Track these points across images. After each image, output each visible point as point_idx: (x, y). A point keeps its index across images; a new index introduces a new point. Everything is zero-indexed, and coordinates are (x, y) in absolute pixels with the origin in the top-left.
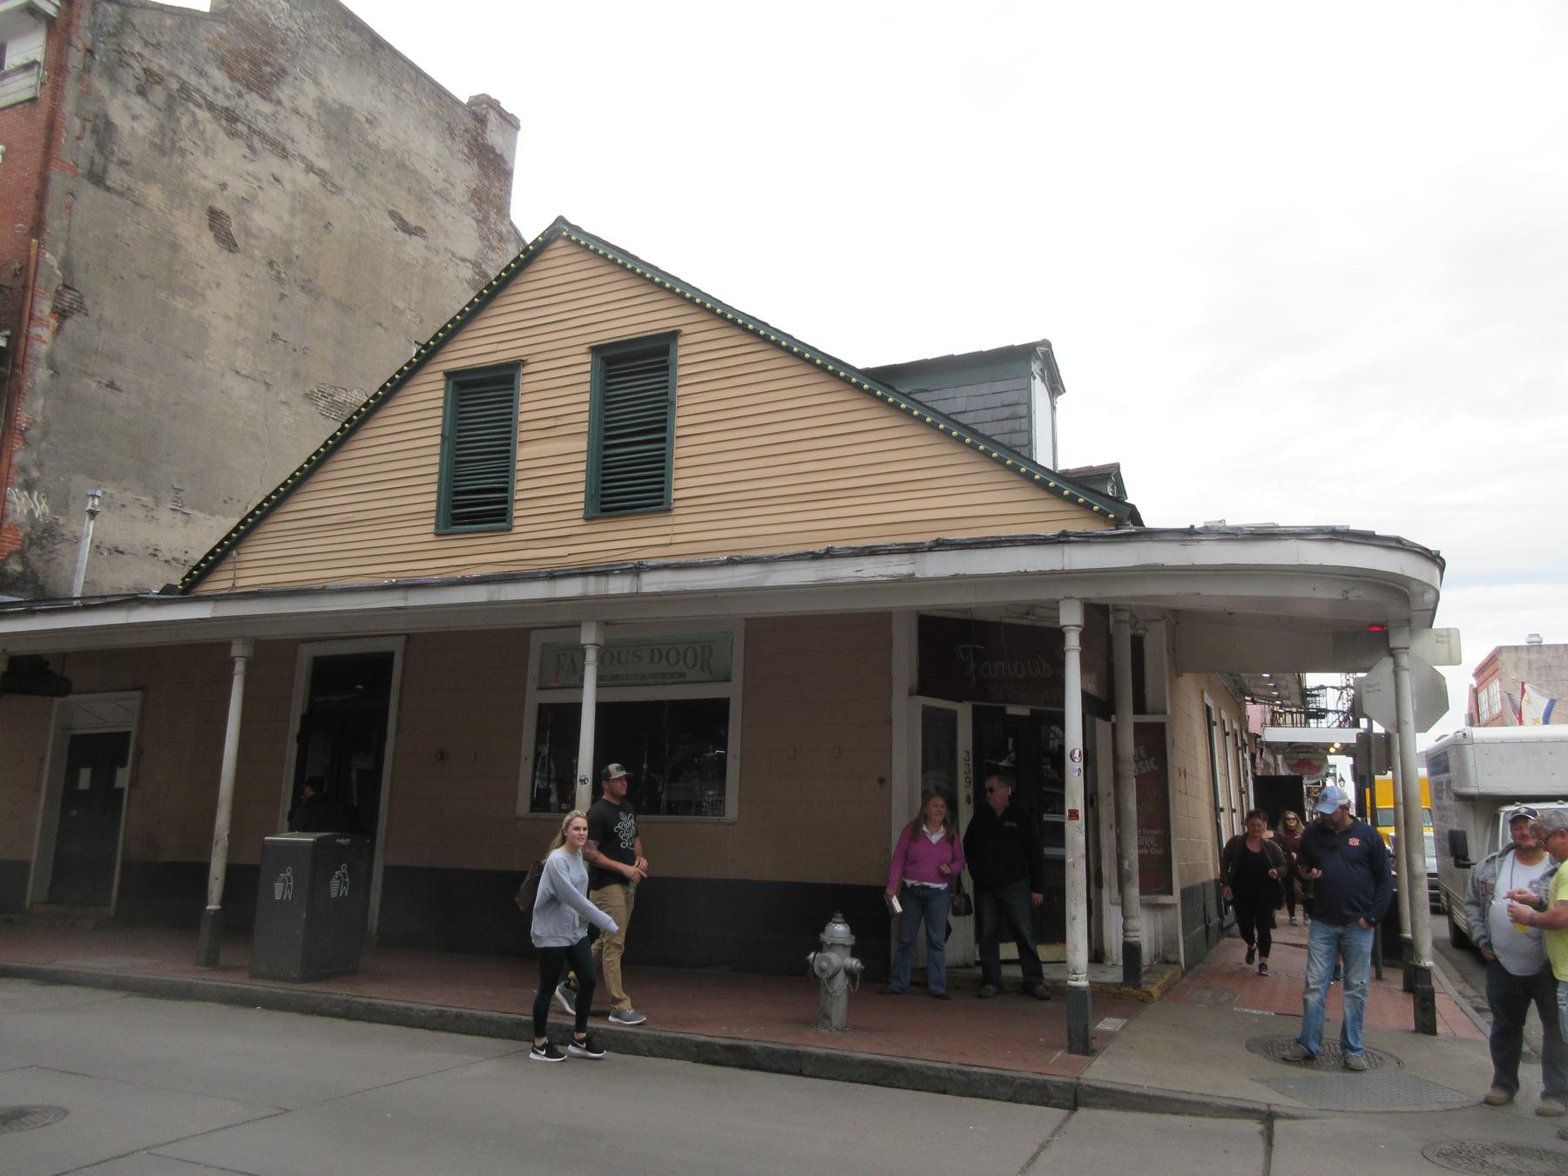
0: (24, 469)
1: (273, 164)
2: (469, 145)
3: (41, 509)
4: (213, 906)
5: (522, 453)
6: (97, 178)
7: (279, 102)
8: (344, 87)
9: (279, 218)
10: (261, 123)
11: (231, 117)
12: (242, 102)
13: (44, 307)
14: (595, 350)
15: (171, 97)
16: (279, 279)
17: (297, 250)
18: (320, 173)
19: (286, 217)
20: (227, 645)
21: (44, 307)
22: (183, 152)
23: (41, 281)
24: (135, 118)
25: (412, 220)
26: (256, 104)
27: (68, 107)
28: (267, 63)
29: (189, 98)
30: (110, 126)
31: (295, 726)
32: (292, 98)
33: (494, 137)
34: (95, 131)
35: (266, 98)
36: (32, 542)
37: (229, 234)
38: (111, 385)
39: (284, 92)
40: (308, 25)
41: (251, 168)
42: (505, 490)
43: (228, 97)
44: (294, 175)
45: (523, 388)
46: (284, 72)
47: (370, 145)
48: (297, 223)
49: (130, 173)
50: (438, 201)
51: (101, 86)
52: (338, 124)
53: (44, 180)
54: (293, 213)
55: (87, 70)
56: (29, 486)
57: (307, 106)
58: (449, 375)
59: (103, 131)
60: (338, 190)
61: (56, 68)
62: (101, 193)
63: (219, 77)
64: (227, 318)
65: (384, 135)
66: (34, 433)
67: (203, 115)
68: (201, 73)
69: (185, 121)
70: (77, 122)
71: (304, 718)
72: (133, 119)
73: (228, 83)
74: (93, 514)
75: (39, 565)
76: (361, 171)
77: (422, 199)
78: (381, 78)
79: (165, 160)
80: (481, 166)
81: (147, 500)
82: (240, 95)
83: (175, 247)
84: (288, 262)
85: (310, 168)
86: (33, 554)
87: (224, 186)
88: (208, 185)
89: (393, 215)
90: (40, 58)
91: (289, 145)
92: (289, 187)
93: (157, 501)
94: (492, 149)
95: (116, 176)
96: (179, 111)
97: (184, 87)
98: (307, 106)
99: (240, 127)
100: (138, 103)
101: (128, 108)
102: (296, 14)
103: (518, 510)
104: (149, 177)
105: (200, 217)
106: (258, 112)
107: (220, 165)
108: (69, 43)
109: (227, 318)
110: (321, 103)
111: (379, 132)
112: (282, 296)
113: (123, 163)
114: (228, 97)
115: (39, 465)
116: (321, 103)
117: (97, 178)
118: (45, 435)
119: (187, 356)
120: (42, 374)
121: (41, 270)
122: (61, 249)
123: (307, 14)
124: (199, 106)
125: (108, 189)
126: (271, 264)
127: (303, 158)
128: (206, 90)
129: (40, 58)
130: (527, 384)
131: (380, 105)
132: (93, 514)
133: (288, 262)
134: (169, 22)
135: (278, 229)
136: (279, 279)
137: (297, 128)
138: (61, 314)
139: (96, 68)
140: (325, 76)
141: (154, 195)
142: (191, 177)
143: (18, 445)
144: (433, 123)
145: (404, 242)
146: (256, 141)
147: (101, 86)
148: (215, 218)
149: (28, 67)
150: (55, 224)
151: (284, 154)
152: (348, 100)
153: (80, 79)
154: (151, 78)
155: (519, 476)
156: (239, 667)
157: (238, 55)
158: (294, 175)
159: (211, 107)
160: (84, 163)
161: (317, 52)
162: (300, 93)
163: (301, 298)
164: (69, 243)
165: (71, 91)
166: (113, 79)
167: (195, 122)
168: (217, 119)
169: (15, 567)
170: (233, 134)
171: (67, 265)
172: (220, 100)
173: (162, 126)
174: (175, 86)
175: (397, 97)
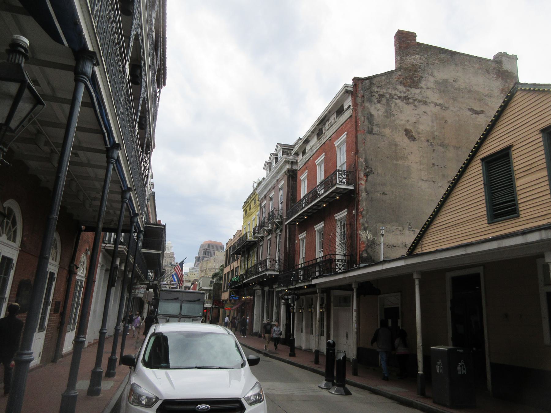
0: (363, 224)
1: (423, 108)
2: (496, 74)
3: (370, 236)
4: (420, 372)
5: (518, 183)
6: (370, 132)
7: (422, 88)
8: (443, 73)
9: (428, 125)
10: (417, 97)
11: (407, 98)
12: (409, 92)
13: (362, 175)
14: (543, 131)
15: (388, 100)
16: (432, 145)
17: (436, 133)
18: (440, 105)
19: (430, 124)
20: (411, 275)
21: (362, 175)
22: (394, 115)
23: (360, 167)
24: (378, 110)
25: (478, 109)
26: (414, 91)
27: (360, 115)
28: (415, 77)
29: (393, 98)
30: (371, 115)
31: (449, 304)
32: (426, 85)
33: (506, 66)
34: (368, 118)
35: (417, 88)
36: (369, 247)
37: (412, 136)
38: (384, 193)
39: (423, 84)
40: (427, 59)
41: (416, 112)
42: (514, 200)
43: (405, 93)
45: (514, 157)
46: (422, 77)
47: (456, 89)
48: (435, 125)
49: (379, 127)
50: (487, 98)
51: (367, 105)
52: (443, 86)
53: (356, 137)
54: (433, 122)
55: (363, 102)
56: (365, 229)
58: (482, 160)
59: (370, 117)
60: (447, 108)
61: (355, 104)
62: (372, 136)
63: (401, 88)
64: (416, 163)
65: (461, 84)
66: (364, 213)
67: (398, 101)
68: (395, 89)
69: (393, 105)
70: (363, 118)
71: (451, 301)
72: (377, 110)
73: (404, 89)
74: (383, 235)
75: (371, 254)
76: (454, 99)
77: (480, 100)
78: (456, 64)
79: (389, 119)
80: (503, 79)
81: (400, 228)
82: (408, 91)
83: (396, 145)
84: (434, 138)
85: (436, 105)
86: (369, 250)
87: (408, 121)
88: (403, 122)
89: (470, 110)
90: (351, 104)
91: (427, 100)
92: (430, 114)
93: (403, 228)
94: (507, 71)
95: (376, 130)
96: (390, 103)
97: (391, 96)
98: (431, 85)
99: (411, 101)
100: (378, 106)
101: (376, 108)
102: (422, 57)
103: (521, 207)
104: (385, 126)
105: (402, 132)
106: (415, 94)
107: (406, 115)
108: (357, 96)
109: (416, 163)
110: (436, 82)
111: (459, 83)
112: (434, 150)
113: (377, 125)
114: (405, 93)
115: (367, 222)
116: (436, 82)
117: (370, 132)
118: (367, 213)
119: (405, 179)
120: (364, 195)
121: (359, 164)
122: (364, 156)
123: (426, 56)
124: (396, 99)
125: (374, 134)
126: (428, 141)
127: (433, 102)
128: (398, 93)
129: (351, 104)
130: (515, 154)
131: (457, 74)
132: (383, 235)
133: (434, 138)
134: (383, 78)
135: (428, 129)
136: (432, 145)
137: (429, 93)
138: (367, 175)
139: (365, 100)
140: (436, 73)
141: (387, 131)
142: (398, 122)
143: (361, 217)
144: (480, 71)
145: (476, 118)
146: (416, 103)
147: (367, 105)
148: (408, 132)
149: (348, 108)
150: (361, 149)
151: (426, 103)
152: (445, 77)
153: (362, 105)
155: (519, 193)
156: (417, 282)
157: (406, 79)
159: (400, 98)
160: (366, 129)
161: (431, 66)
162: (428, 82)
163: (441, 149)
164: (366, 155)
165: (359, 109)
166: (370, 101)
167: (396, 104)
168: (403, 101)
169: (365, 255)
170: (408, 104)
171: (366, 160)
172: (403, 95)
173: (386, 110)
174: (388, 96)
175: (463, 69)
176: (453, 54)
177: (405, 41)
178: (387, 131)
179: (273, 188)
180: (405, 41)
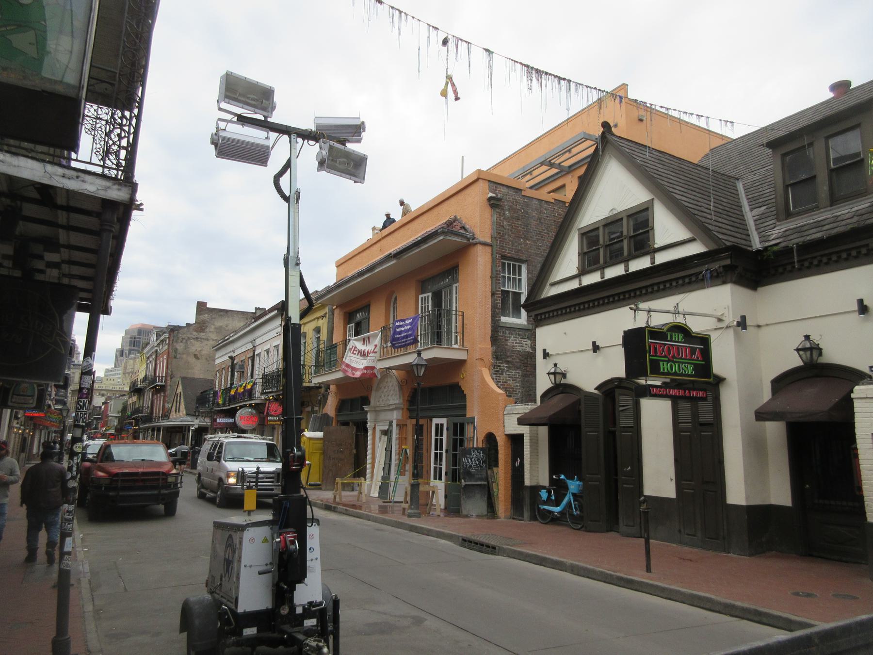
1: (206, 342)
6: (175, 357)
8: (220, 323)
11: (197, 338)
39: (207, 330)
52: (219, 330)
57: (212, 330)
59: (176, 350)
63: (195, 333)
72: (180, 347)
95: (178, 356)
98: (212, 330)
107: (195, 347)
110: (215, 328)
117: (175, 357)
120: (169, 387)
151: (208, 340)
162: (212, 328)
166: (177, 342)
177: (201, 307)
178: (184, 356)
179: (151, 355)
180: (201, 307)
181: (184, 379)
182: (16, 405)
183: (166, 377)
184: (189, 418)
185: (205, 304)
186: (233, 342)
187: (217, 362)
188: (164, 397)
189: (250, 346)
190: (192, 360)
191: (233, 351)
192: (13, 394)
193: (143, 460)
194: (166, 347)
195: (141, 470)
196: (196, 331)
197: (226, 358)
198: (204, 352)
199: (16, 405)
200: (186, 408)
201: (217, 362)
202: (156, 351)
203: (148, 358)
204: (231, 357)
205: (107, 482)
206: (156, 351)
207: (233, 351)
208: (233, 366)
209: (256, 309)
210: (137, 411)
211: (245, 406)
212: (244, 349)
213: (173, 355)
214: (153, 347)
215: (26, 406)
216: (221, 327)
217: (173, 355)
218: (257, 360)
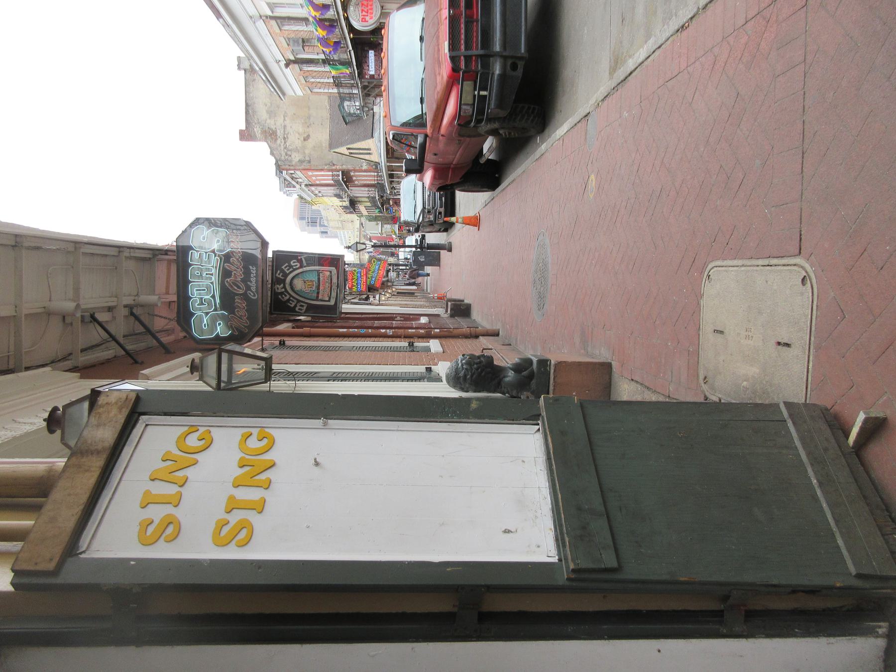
1: (288, 128)
6: (309, 162)
8: (262, 113)
11: (284, 138)
39: (273, 127)
44: (288, 122)
52: (272, 114)
57: (272, 122)
59: (301, 162)
63: (279, 142)
72: (296, 157)
95: (307, 158)
97: (285, 148)
98: (272, 122)
107: (295, 140)
117: (309, 162)
120: (344, 167)
150: (320, 168)
151: (285, 127)
154: (286, 154)
158: (288, 122)
162: (271, 123)
166: (291, 161)
176: (247, 105)
177: (246, 135)
178: (307, 152)
179: (312, 192)
180: (246, 135)
181: (331, 146)
182: (334, 294)
183: (332, 171)
184: (376, 135)
185: (241, 132)
186: (265, 64)
187: (299, 93)
188: (355, 171)
189: (260, 24)
190: (310, 143)
191: (278, 62)
192: (317, 299)
193: (421, 39)
194: (298, 173)
195: (445, 13)
196: (276, 140)
197: (288, 71)
198: (301, 130)
199: (334, 294)
200: (365, 138)
201: (299, 93)
202: (306, 185)
203: (316, 195)
204: (287, 65)
205: (468, 85)
206: (306, 185)
207: (278, 62)
208: (297, 61)
209: (239, 68)
210: (372, 200)
211: (347, 19)
212: (270, 41)
213: (307, 165)
214: (303, 191)
215: (335, 280)
216: (268, 112)
217: (307, 165)
218: (281, 12)
